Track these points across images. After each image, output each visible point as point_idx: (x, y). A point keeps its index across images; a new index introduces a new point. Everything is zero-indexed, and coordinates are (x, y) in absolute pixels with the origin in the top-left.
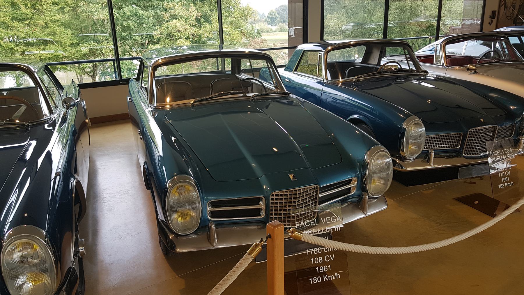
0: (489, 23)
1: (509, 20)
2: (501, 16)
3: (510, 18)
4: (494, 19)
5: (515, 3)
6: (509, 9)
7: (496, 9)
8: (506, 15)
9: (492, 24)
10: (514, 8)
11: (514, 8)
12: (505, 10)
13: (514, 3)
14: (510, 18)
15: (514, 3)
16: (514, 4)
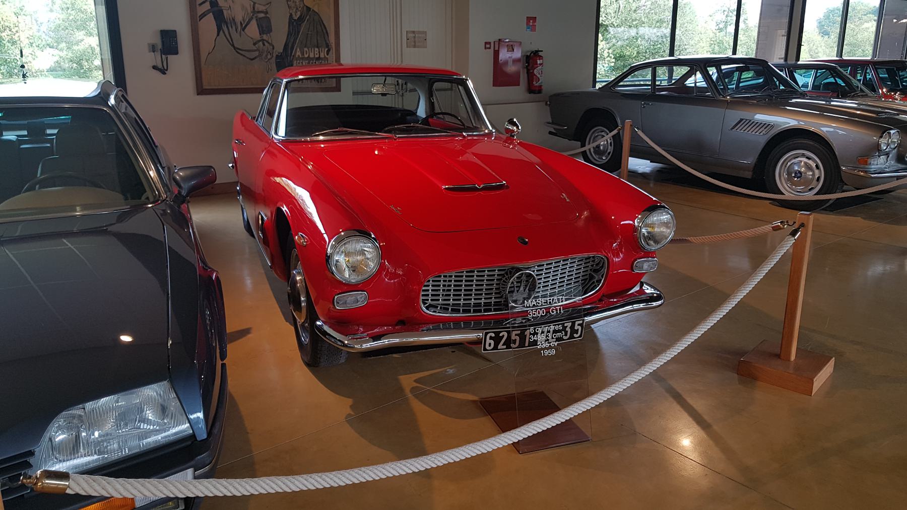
0: (155, 67)
1: (252, 59)
2: (205, 49)
3: (257, 53)
4: (171, 58)
5: (266, 13)
6: (243, 30)
7: (181, 25)
8: (233, 45)
9: (167, 70)
10: (265, 27)
11: (265, 27)
12: (219, 29)
13: (259, 12)
14: (257, 53)
15: (259, 12)
16: (262, 15)
